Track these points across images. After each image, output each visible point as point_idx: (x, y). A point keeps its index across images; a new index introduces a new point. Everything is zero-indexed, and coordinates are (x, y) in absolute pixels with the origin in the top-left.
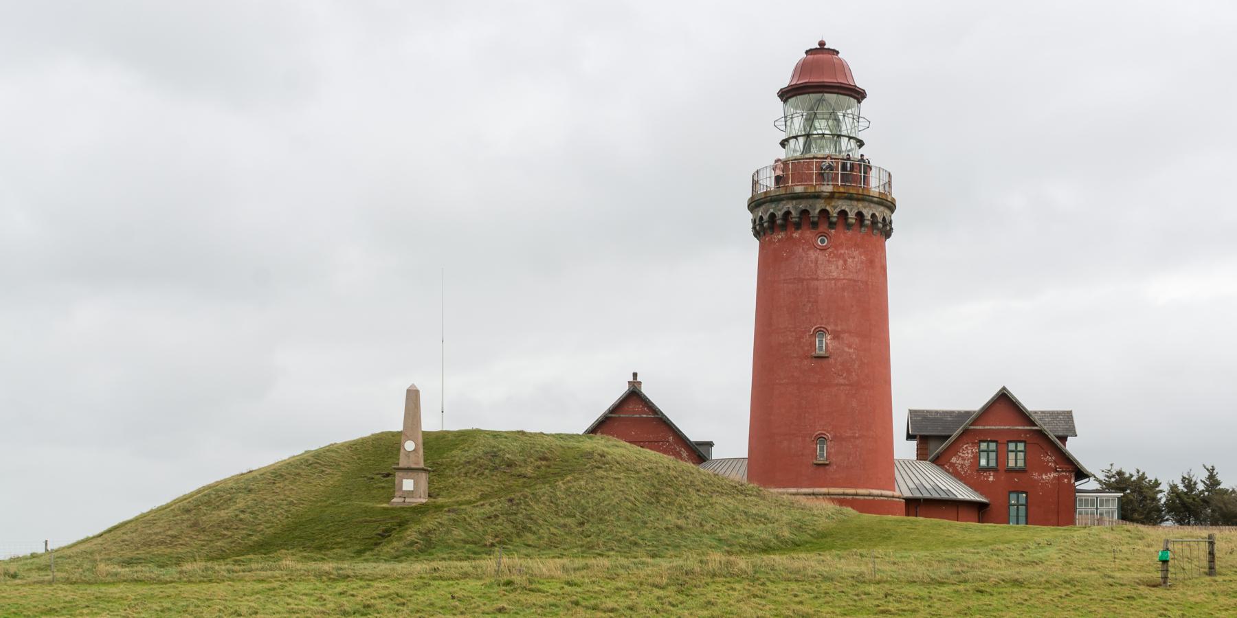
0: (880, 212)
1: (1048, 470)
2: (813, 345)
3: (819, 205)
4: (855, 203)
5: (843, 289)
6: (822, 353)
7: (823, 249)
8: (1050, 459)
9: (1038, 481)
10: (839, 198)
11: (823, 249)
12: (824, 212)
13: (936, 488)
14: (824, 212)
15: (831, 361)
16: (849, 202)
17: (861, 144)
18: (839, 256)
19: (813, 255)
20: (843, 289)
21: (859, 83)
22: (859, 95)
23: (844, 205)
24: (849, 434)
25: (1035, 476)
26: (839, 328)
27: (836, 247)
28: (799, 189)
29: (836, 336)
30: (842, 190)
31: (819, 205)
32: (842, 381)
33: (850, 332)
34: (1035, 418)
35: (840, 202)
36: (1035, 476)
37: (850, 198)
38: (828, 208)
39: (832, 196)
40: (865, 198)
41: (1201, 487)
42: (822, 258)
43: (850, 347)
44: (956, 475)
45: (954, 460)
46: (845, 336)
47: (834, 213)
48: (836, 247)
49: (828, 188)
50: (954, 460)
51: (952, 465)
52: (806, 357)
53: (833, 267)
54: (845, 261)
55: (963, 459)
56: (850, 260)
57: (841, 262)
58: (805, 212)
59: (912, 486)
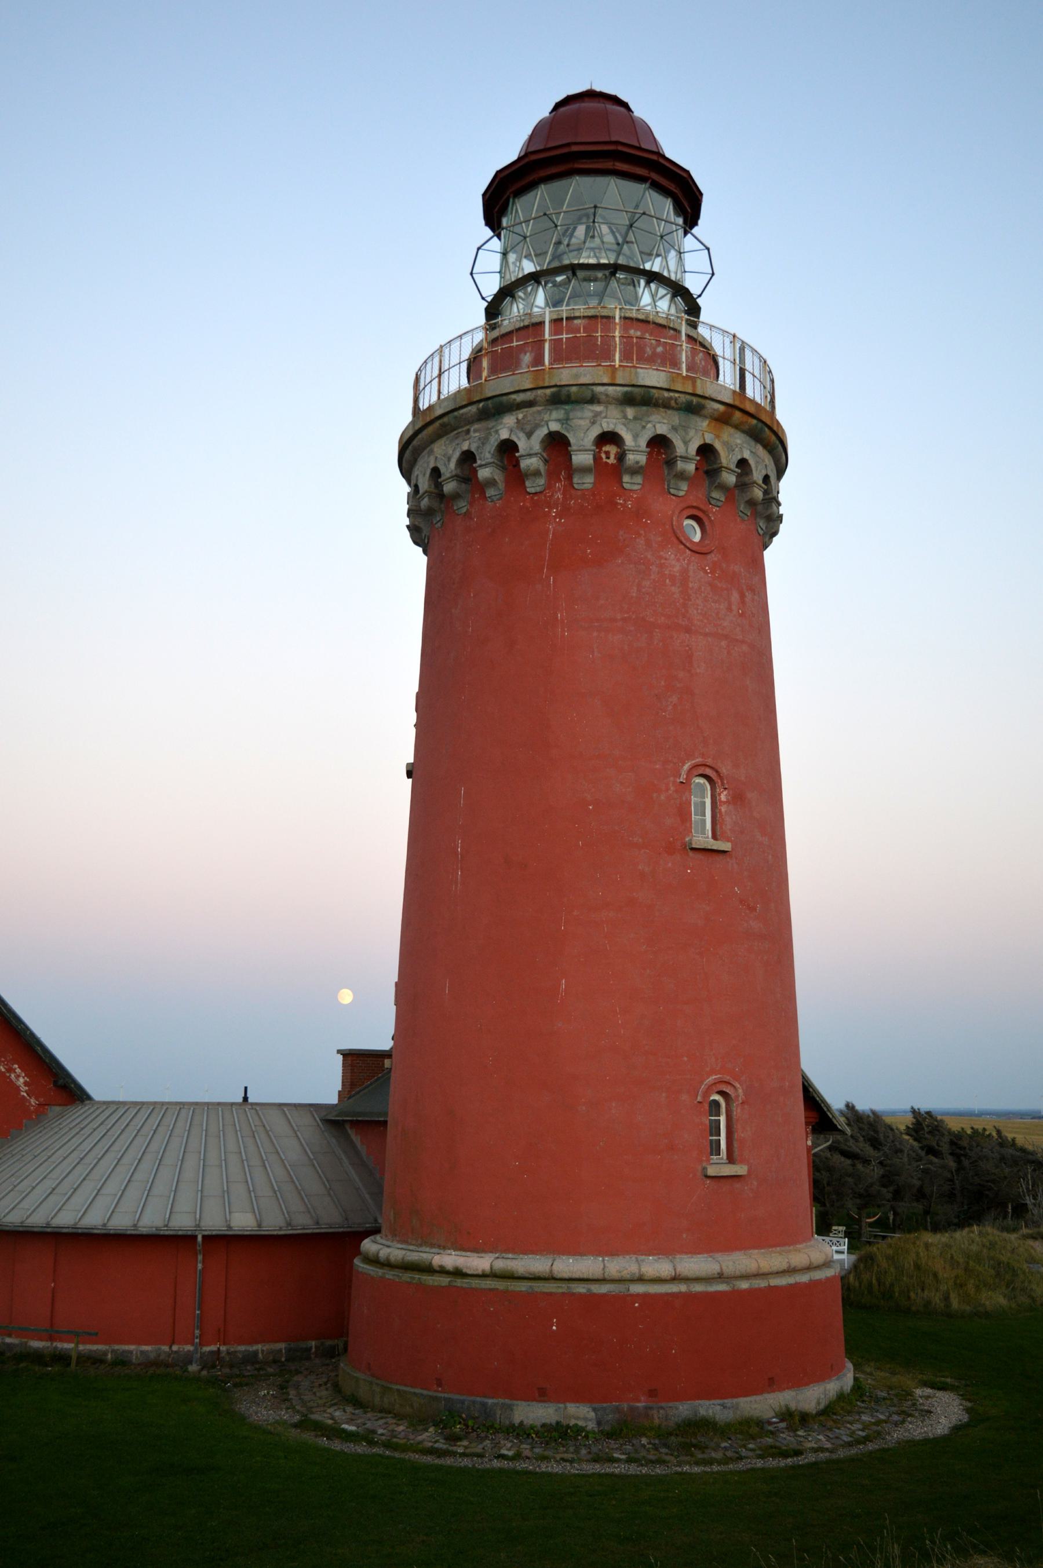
2: (684, 814)
4: (760, 450)
7: (698, 551)
10: (736, 427)
11: (698, 551)
12: (706, 451)
14: (706, 451)
16: (753, 443)
19: (674, 561)
28: (652, 377)
29: (738, 798)
35: (739, 439)
38: (718, 446)
47: (727, 459)
52: (670, 849)
56: (749, 595)
57: (735, 596)
58: (659, 443)
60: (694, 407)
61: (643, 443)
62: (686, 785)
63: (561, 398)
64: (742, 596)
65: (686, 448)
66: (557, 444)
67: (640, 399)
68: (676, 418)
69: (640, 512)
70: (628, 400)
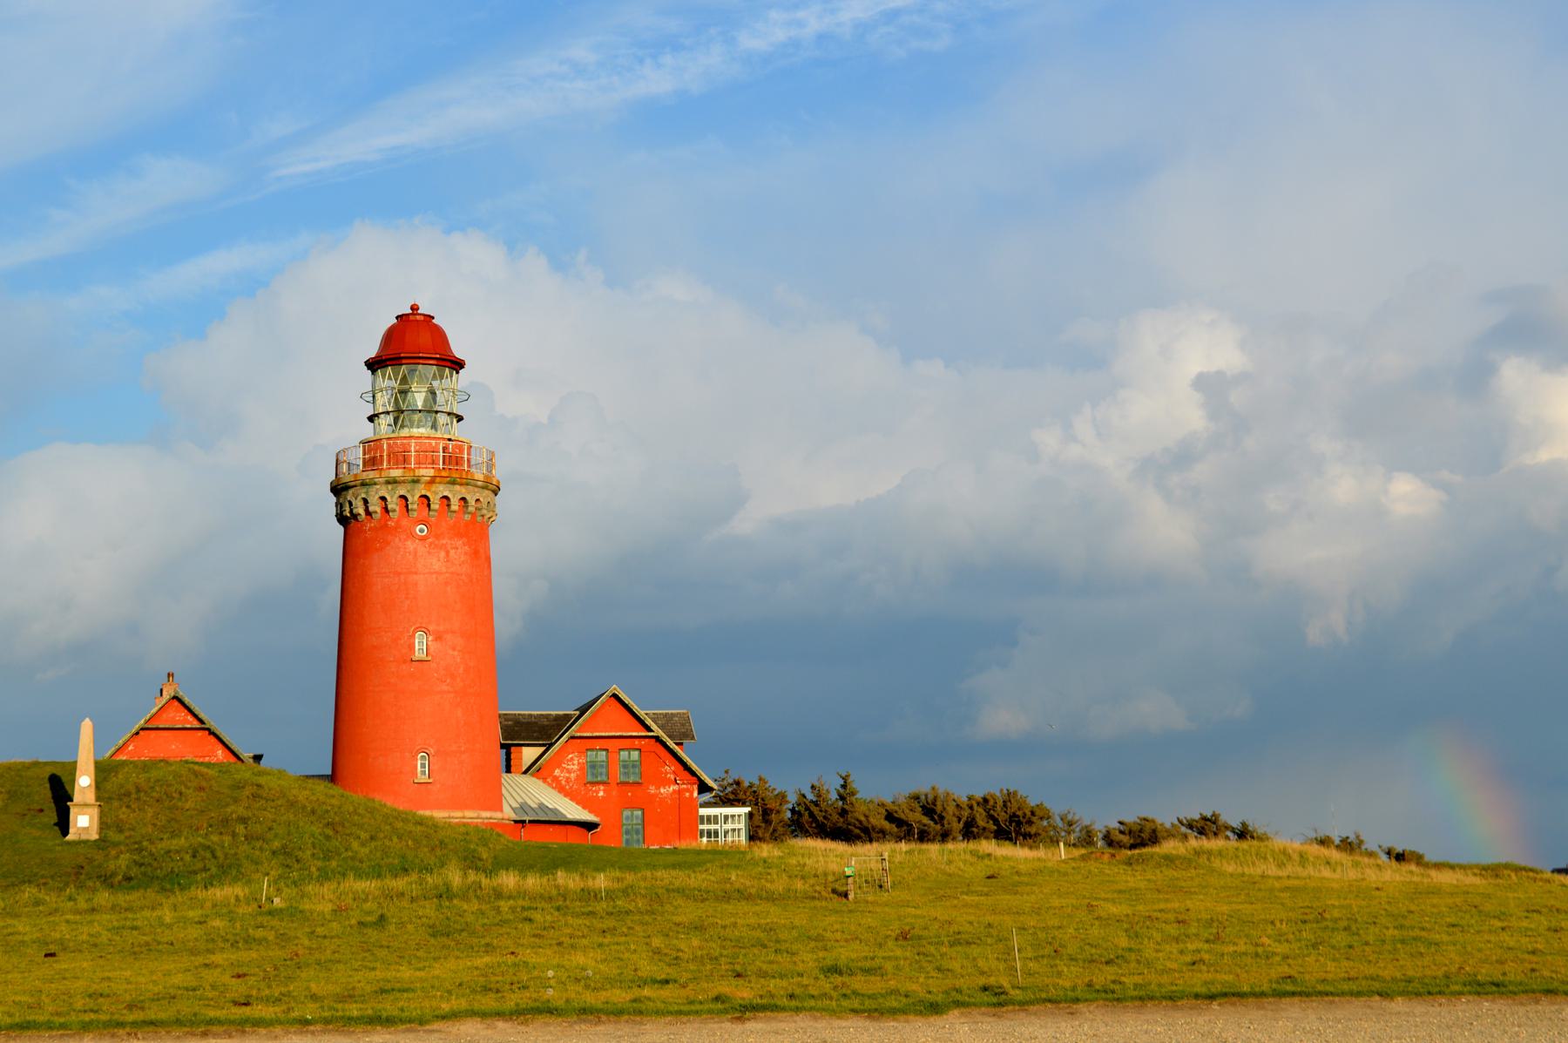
0: (485, 496)
1: (667, 783)
3: (421, 490)
4: (457, 487)
5: (446, 584)
6: (423, 656)
8: (670, 768)
9: (655, 795)
11: (423, 539)
13: (542, 807)
15: (433, 665)
17: (460, 419)
18: (443, 547)
20: (446, 584)
21: (458, 351)
22: (458, 365)
23: (443, 490)
24: (454, 748)
25: (652, 790)
26: (441, 628)
27: (437, 537)
28: (396, 473)
30: (444, 474)
31: (421, 490)
32: (445, 688)
33: (453, 632)
34: (649, 722)
35: (441, 487)
36: (652, 790)
37: (454, 483)
39: (432, 481)
40: (467, 482)
41: (834, 796)
42: (422, 549)
43: (454, 649)
44: (561, 790)
45: (557, 772)
46: (448, 637)
48: (437, 537)
49: (431, 472)
50: (557, 772)
51: (556, 779)
53: (434, 561)
54: (447, 553)
55: (569, 771)
56: (452, 552)
57: (443, 554)
59: (515, 805)
60: (416, 481)
61: (395, 499)
62: (413, 636)
63: (364, 484)
64: (447, 553)
65: (414, 499)
66: (365, 501)
67: (393, 482)
68: (409, 486)
69: (398, 526)
70: (388, 483)
